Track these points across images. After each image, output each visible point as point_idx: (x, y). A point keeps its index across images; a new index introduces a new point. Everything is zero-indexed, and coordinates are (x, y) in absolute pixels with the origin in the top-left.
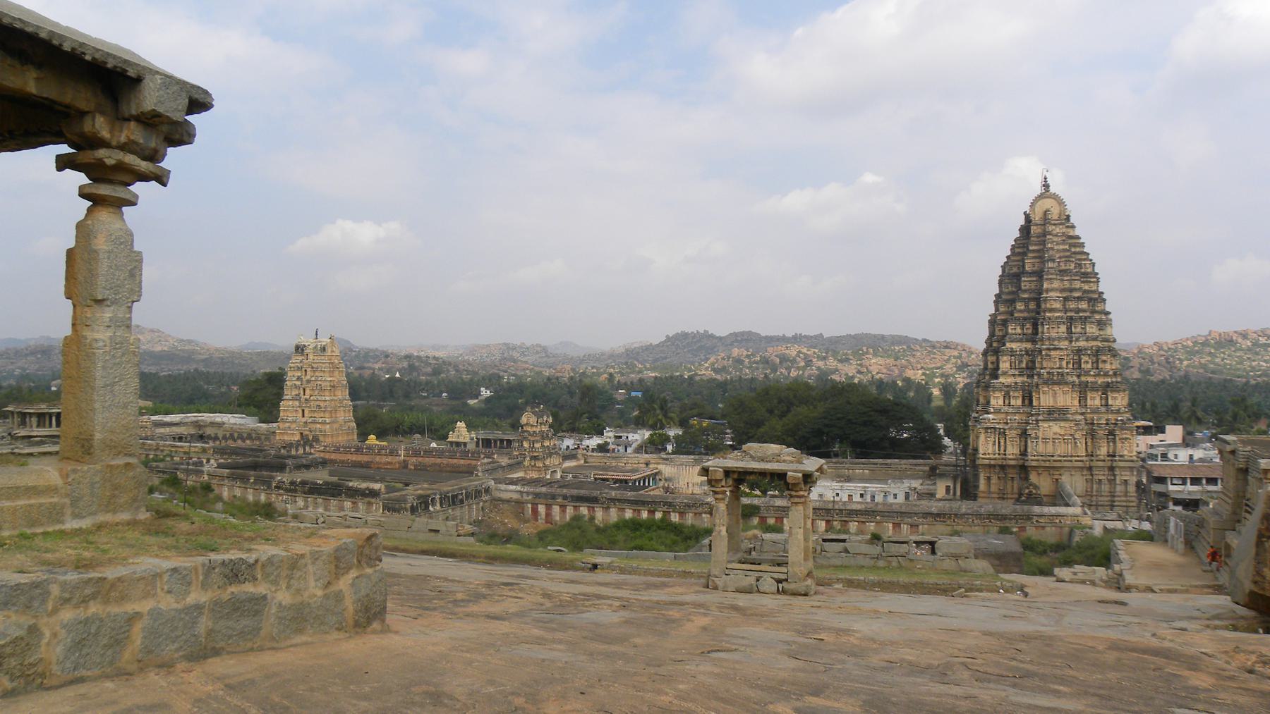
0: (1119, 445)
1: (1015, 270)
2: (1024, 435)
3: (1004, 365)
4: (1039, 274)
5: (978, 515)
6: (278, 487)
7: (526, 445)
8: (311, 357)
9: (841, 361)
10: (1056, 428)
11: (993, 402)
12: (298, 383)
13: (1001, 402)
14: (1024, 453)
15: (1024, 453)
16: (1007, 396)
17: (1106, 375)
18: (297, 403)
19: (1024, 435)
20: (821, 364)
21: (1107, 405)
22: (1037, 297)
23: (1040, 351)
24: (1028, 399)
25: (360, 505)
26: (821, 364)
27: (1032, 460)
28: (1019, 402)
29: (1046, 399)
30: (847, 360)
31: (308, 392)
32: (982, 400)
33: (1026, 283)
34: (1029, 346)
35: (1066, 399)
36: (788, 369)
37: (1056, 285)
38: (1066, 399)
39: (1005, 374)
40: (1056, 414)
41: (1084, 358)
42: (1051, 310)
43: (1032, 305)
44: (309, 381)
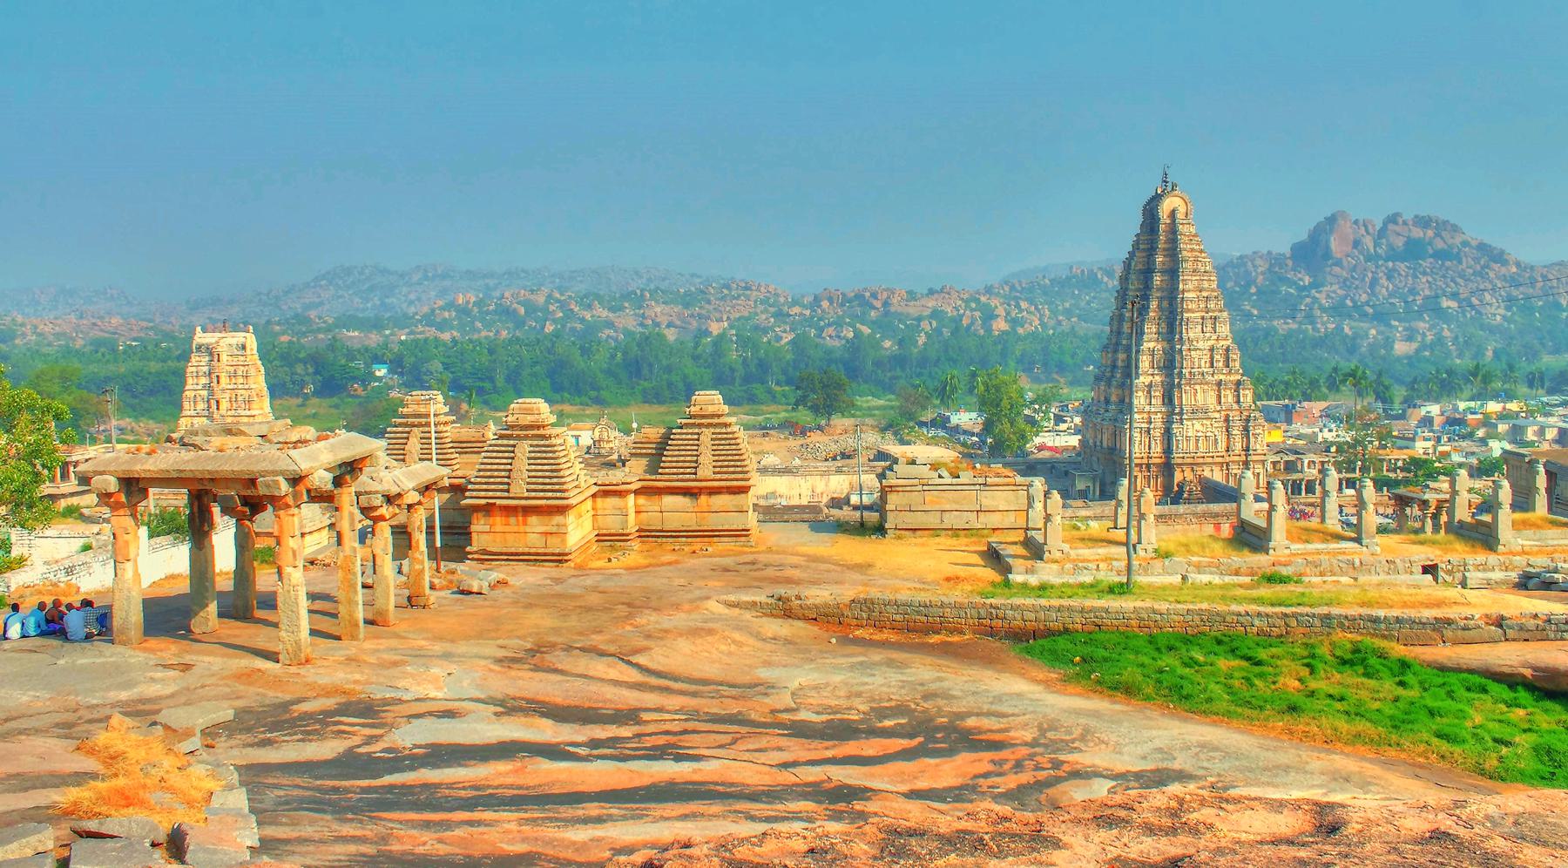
0: (1252, 440)
1: (1140, 266)
2: (1168, 434)
3: (1145, 362)
4: (1173, 273)
5: (1194, 514)
9: (612, 309)
10: (1198, 426)
11: (1136, 402)
14: (1168, 451)
15: (1168, 451)
17: (1237, 372)
19: (1168, 434)
21: (1238, 402)
22: (1172, 298)
24: (1168, 399)
27: (1177, 458)
28: (1160, 401)
29: (1189, 398)
30: (622, 308)
32: (1113, 398)
33: (1157, 279)
34: (1165, 344)
37: (1190, 286)
39: (1146, 373)
40: (1200, 412)
41: (1217, 357)
42: (1189, 311)
43: (1165, 304)
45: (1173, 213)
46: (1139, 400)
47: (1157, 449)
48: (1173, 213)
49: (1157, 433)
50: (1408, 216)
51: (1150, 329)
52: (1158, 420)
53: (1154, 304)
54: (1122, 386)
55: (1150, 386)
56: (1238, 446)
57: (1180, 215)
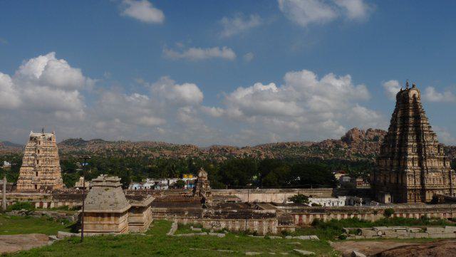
2: (422, 178)
3: (410, 151)
6: (206, 216)
7: (203, 187)
8: (42, 143)
10: (433, 174)
12: (33, 157)
13: (411, 164)
14: (422, 184)
15: (422, 184)
16: (413, 163)
18: (32, 169)
19: (422, 178)
20: (145, 152)
23: (425, 146)
24: (420, 165)
25: (264, 223)
26: (145, 152)
31: (40, 162)
33: (411, 120)
35: (436, 164)
36: (132, 154)
38: (436, 164)
39: (410, 154)
40: (434, 170)
44: (41, 156)
45: (414, 95)
46: (410, 164)
47: (418, 183)
48: (414, 95)
49: (418, 177)
50: (374, 129)
51: (410, 138)
52: (418, 171)
53: (410, 129)
54: (399, 159)
55: (413, 159)
56: (448, 182)
57: (417, 96)
